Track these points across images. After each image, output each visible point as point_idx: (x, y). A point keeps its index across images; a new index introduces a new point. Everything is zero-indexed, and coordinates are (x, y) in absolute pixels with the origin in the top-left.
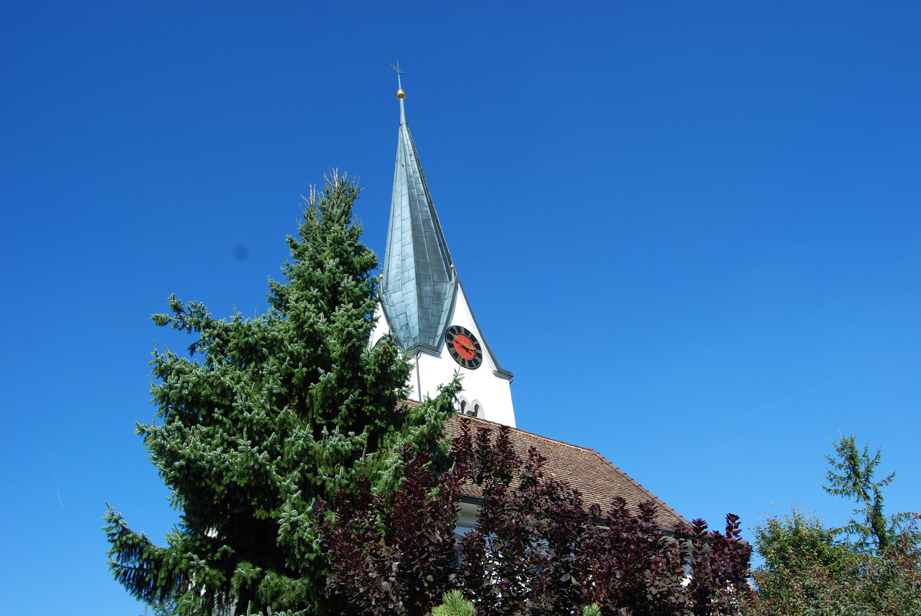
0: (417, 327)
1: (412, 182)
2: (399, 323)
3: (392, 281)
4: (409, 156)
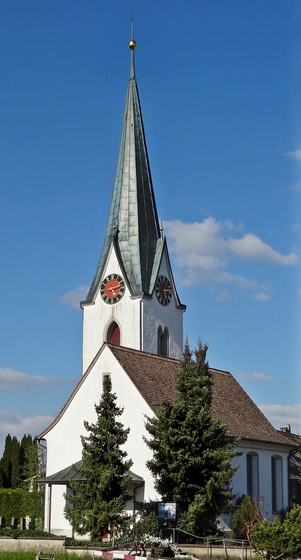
0: (140, 277)
3: (121, 231)
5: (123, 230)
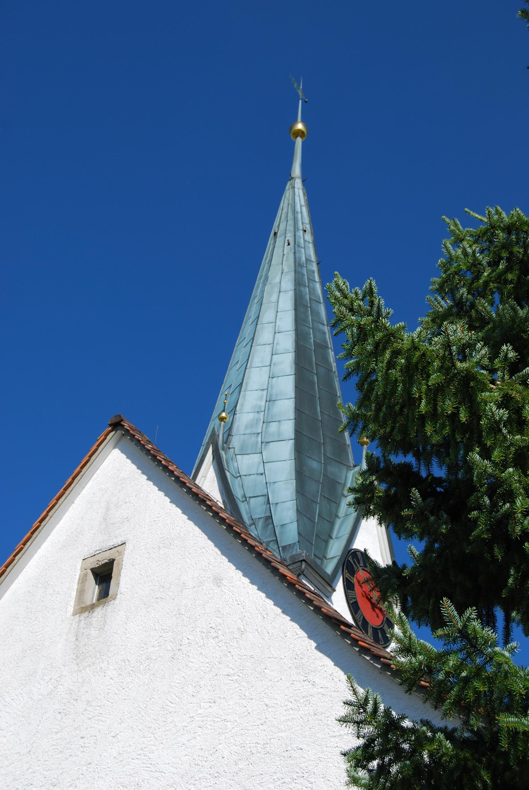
0: (293, 528)
1: (303, 275)
2: (249, 513)
4: (301, 232)
5: (248, 431)
